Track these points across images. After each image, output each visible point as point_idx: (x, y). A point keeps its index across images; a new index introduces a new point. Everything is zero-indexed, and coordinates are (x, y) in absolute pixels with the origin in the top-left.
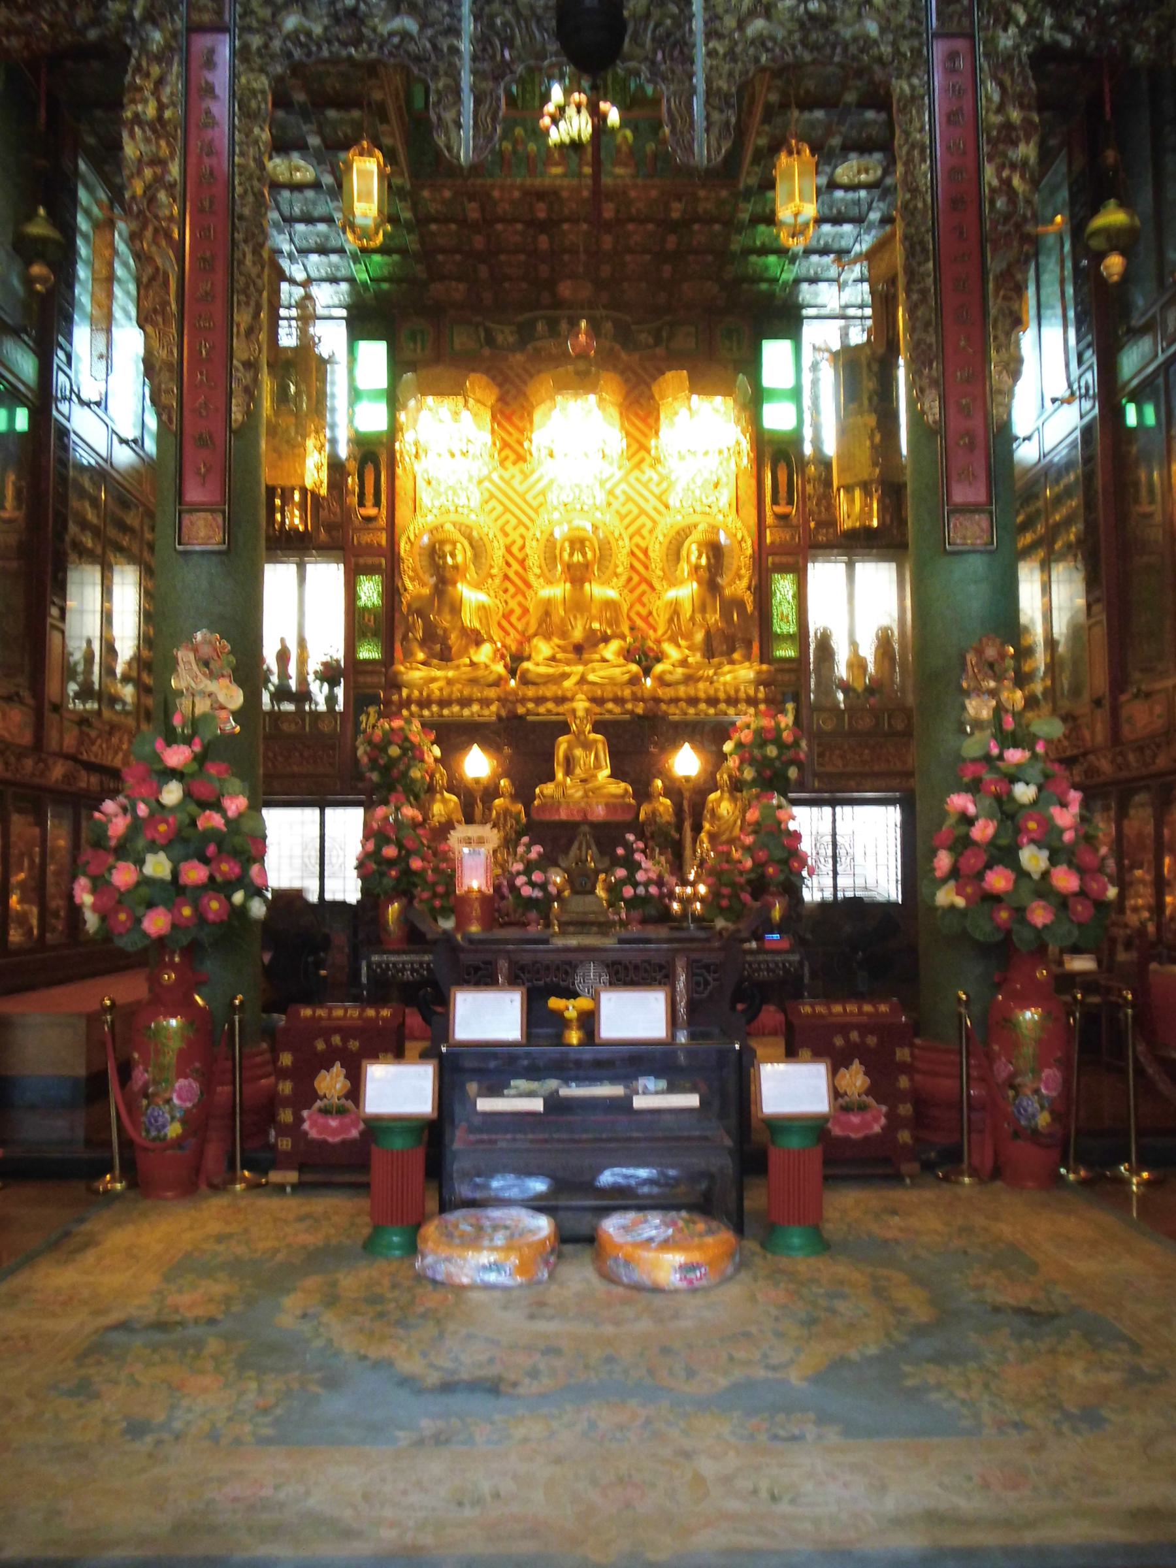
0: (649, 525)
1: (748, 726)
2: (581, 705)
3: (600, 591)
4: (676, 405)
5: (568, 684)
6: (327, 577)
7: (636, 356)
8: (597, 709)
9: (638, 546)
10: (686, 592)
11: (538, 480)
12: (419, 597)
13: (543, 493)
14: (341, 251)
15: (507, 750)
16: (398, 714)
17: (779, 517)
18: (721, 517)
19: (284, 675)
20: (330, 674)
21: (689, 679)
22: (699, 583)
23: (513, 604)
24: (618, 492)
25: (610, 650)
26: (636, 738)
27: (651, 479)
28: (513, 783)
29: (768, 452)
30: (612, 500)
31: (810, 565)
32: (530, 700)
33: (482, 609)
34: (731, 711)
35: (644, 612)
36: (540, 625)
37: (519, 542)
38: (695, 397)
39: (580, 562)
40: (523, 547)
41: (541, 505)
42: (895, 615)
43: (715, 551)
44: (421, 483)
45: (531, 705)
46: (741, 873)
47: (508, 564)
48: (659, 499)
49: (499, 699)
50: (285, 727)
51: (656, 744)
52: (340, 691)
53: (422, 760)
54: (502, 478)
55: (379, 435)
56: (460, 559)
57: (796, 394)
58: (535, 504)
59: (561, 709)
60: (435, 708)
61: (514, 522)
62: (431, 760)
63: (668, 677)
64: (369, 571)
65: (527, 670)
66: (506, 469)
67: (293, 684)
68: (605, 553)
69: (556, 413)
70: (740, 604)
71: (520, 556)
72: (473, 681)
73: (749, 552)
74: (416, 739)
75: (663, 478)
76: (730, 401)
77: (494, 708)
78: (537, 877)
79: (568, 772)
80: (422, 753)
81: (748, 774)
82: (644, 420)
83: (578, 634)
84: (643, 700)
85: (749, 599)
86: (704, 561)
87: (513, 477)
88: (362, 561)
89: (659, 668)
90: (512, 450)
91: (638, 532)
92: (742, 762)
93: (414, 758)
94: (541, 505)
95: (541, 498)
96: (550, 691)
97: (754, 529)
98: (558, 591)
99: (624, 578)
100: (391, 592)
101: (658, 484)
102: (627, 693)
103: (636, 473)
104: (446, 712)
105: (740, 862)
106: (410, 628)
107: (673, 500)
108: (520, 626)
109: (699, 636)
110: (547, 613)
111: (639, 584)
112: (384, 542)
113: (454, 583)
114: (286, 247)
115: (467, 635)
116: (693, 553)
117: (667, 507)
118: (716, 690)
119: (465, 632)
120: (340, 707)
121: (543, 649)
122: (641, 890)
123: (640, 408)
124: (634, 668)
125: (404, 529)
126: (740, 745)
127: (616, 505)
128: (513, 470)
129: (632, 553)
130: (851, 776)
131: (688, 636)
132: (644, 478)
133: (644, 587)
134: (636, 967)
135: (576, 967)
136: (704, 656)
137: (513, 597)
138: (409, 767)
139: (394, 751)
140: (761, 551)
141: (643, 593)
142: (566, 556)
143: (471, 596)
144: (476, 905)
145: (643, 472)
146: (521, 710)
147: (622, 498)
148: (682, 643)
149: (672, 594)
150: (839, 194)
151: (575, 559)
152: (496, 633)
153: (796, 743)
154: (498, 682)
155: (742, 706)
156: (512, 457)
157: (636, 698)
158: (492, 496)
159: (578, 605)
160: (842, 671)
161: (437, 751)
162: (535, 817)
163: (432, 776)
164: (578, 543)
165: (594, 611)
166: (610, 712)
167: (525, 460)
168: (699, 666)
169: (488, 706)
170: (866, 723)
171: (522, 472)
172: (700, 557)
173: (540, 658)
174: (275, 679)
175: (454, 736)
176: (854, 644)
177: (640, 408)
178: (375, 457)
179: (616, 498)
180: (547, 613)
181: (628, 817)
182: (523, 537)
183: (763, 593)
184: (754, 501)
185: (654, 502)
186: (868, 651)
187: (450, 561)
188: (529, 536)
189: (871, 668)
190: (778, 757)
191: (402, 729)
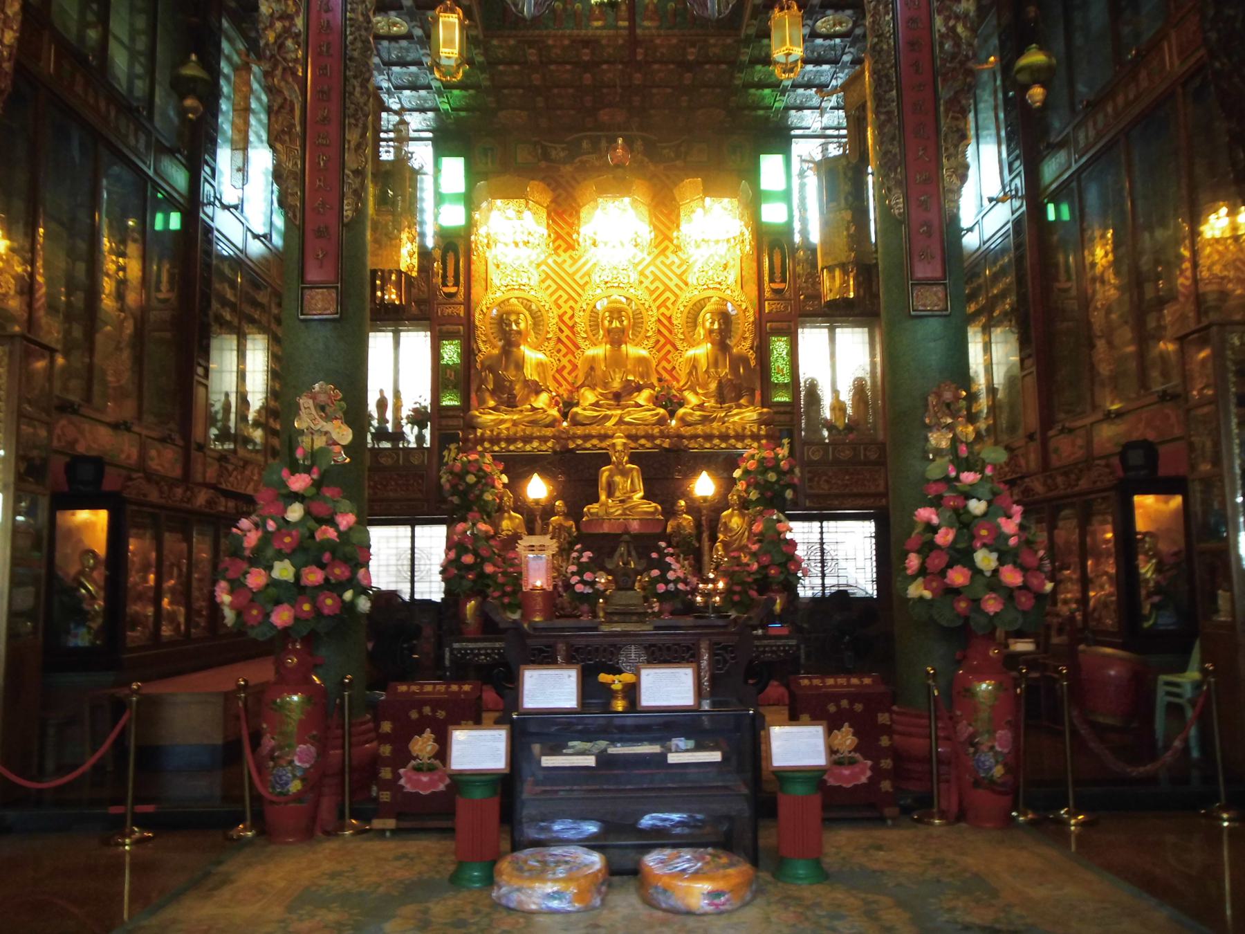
0: (673, 298)
1: (753, 456)
2: (619, 441)
3: (634, 351)
4: (694, 204)
5: (609, 424)
6: (417, 342)
7: (662, 167)
8: (633, 445)
9: (663, 314)
10: (702, 351)
11: (585, 264)
12: (490, 357)
13: (588, 274)
14: (428, 87)
15: (561, 478)
16: (473, 450)
17: (775, 291)
18: (728, 292)
19: (383, 420)
20: (419, 418)
21: (705, 420)
23: (565, 361)
24: (647, 272)
25: (643, 397)
26: (664, 466)
27: (673, 262)
28: (566, 504)
29: (766, 240)
31: (800, 330)
33: (540, 365)
34: (739, 445)
35: (669, 367)
36: (586, 378)
37: (570, 313)
38: (707, 199)
39: (618, 327)
40: (572, 317)
41: (587, 283)
42: (868, 368)
43: (725, 318)
44: (491, 268)
45: (579, 442)
46: (750, 574)
47: (562, 331)
48: (680, 276)
49: (554, 437)
50: (383, 461)
51: (679, 471)
52: (427, 432)
53: (493, 487)
54: (555, 262)
55: (459, 228)
56: (522, 326)
57: (787, 196)
58: (582, 282)
59: (604, 445)
60: (503, 445)
61: (565, 297)
62: (500, 486)
63: (689, 419)
64: (450, 336)
65: (577, 413)
66: (559, 255)
67: (390, 427)
68: (638, 320)
69: (598, 212)
70: (744, 360)
71: (570, 324)
72: (533, 423)
73: (752, 319)
74: (488, 470)
75: (683, 262)
76: (735, 202)
77: (550, 444)
78: (588, 576)
79: (610, 494)
80: (493, 481)
81: (754, 495)
82: (668, 216)
83: (616, 385)
84: (668, 437)
85: (751, 355)
86: (716, 326)
87: (565, 261)
88: (445, 328)
89: (681, 411)
90: (563, 240)
91: (663, 304)
92: (748, 486)
93: (486, 484)
94: (587, 283)
95: (586, 278)
96: (595, 430)
97: (756, 301)
98: (600, 351)
99: (652, 341)
100: (468, 353)
101: (679, 267)
102: (656, 431)
103: (662, 258)
104: (512, 448)
105: (748, 565)
106: (483, 381)
107: (692, 280)
108: (570, 379)
109: (713, 386)
110: (592, 368)
111: (664, 345)
112: (462, 314)
113: (518, 346)
114: (385, 85)
115: (529, 386)
116: (707, 320)
117: (686, 284)
118: (728, 428)
119: (526, 383)
120: (427, 444)
121: (589, 396)
122: (671, 586)
123: (665, 209)
124: (662, 411)
125: (478, 303)
126: (746, 472)
127: (647, 283)
128: (565, 256)
129: (659, 320)
130: (837, 496)
132: (668, 262)
133: (669, 347)
134: (669, 649)
135: (620, 648)
136: (717, 402)
137: (564, 356)
138: (482, 492)
139: (471, 479)
140: (761, 320)
141: (669, 352)
142: (606, 323)
143: (531, 355)
144: (539, 599)
145: (667, 257)
146: (572, 446)
147: (651, 278)
148: (700, 391)
149: (691, 353)
150: (819, 41)
151: (614, 325)
152: (551, 385)
153: (791, 471)
154: (552, 424)
155: (748, 441)
156: (564, 246)
157: (663, 435)
158: (548, 276)
159: (616, 361)
160: (827, 413)
161: (505, 479)
162: (584, 531)
163: (501, 499)
164: (616, 313)
165: (629, 367)
166: (643, 446)
167: (574, 249)
168: (714, 409)
170: (847, 454)
171: (571, 257)
172: (712, 323)
173: (587, 404)
174: (375, 423)
175: (519, 467)
176: (835, 392)
177: (665, 209)
178: (456, 248)
179: (647, 277)
180: (592, 368)
181: (659, 530)
182: (571, 307)
183: (763, 352)
184: (755, 276)
186: (846, 396)
187: (514, 327)
188: (577, 307)
189: (849, 411)
190: (777, 482)
191: (477, 460)
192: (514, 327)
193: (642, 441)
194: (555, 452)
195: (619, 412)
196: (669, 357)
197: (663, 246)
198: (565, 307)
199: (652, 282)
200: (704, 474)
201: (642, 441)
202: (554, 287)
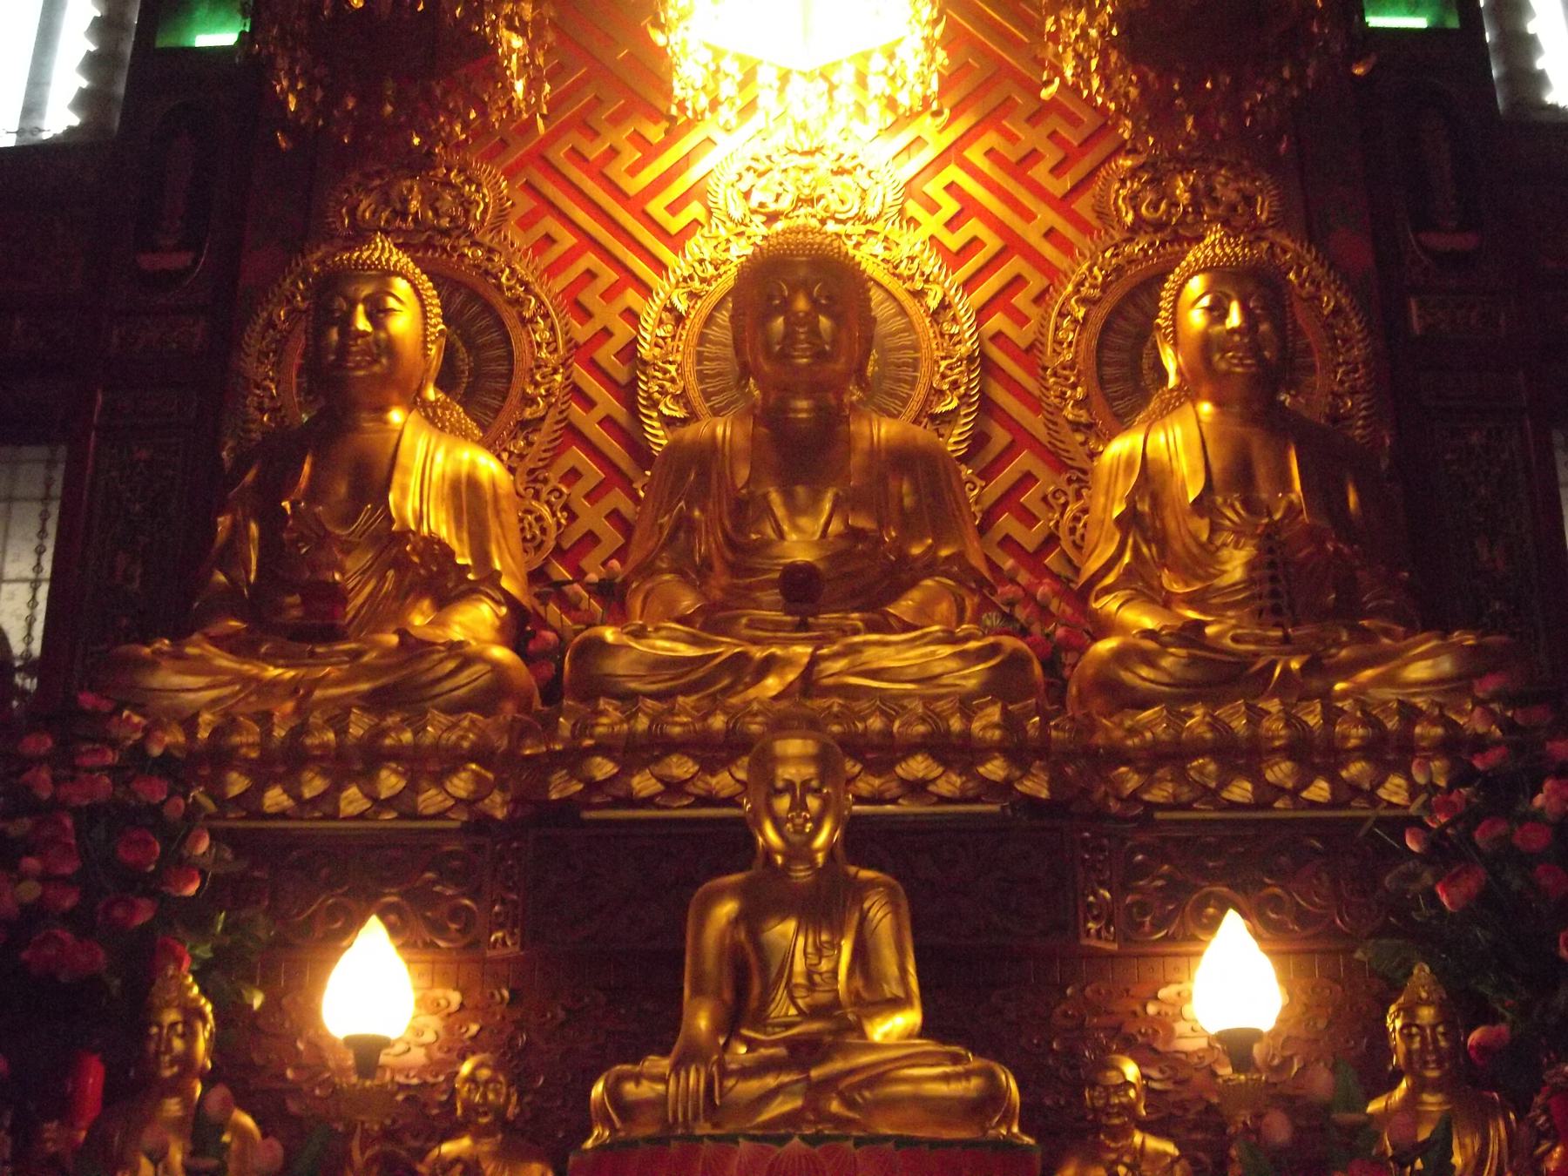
0: (1036, 282)
22: (1218, 403)
23: (592, 518)
30: (913, 209)
32: (604, 748)
35: (1030, 538)
45: (603, 768)
49: (481, 754)
51: (1107, 916)
59: (723, 782)
77: (460, 785)
79: (739, 1014)
86: (1234, 319)
95: (695, 210)
109: (1235, 564)
115: (401, 564)
131: (1202, 562)
137: (593, 496)
141: (1028, 479)
146: (561, 787)
147: (950, 207)
149: (1123, 446)
166: (917, 788)
169: (439, 780)
172: (1217, 311)
179: (933, 208)
185: (1047, 216)
187: (362, 324)
188: (650, 312)
192: (362, 324)
193: (918, 766)
194: (481, 824)
195: (803, 651)
196: (1028, 498)
197: (994, 99)
198: (607, 315)
199: (952, 224)
200: (1233, 925)
201: (918, 766)
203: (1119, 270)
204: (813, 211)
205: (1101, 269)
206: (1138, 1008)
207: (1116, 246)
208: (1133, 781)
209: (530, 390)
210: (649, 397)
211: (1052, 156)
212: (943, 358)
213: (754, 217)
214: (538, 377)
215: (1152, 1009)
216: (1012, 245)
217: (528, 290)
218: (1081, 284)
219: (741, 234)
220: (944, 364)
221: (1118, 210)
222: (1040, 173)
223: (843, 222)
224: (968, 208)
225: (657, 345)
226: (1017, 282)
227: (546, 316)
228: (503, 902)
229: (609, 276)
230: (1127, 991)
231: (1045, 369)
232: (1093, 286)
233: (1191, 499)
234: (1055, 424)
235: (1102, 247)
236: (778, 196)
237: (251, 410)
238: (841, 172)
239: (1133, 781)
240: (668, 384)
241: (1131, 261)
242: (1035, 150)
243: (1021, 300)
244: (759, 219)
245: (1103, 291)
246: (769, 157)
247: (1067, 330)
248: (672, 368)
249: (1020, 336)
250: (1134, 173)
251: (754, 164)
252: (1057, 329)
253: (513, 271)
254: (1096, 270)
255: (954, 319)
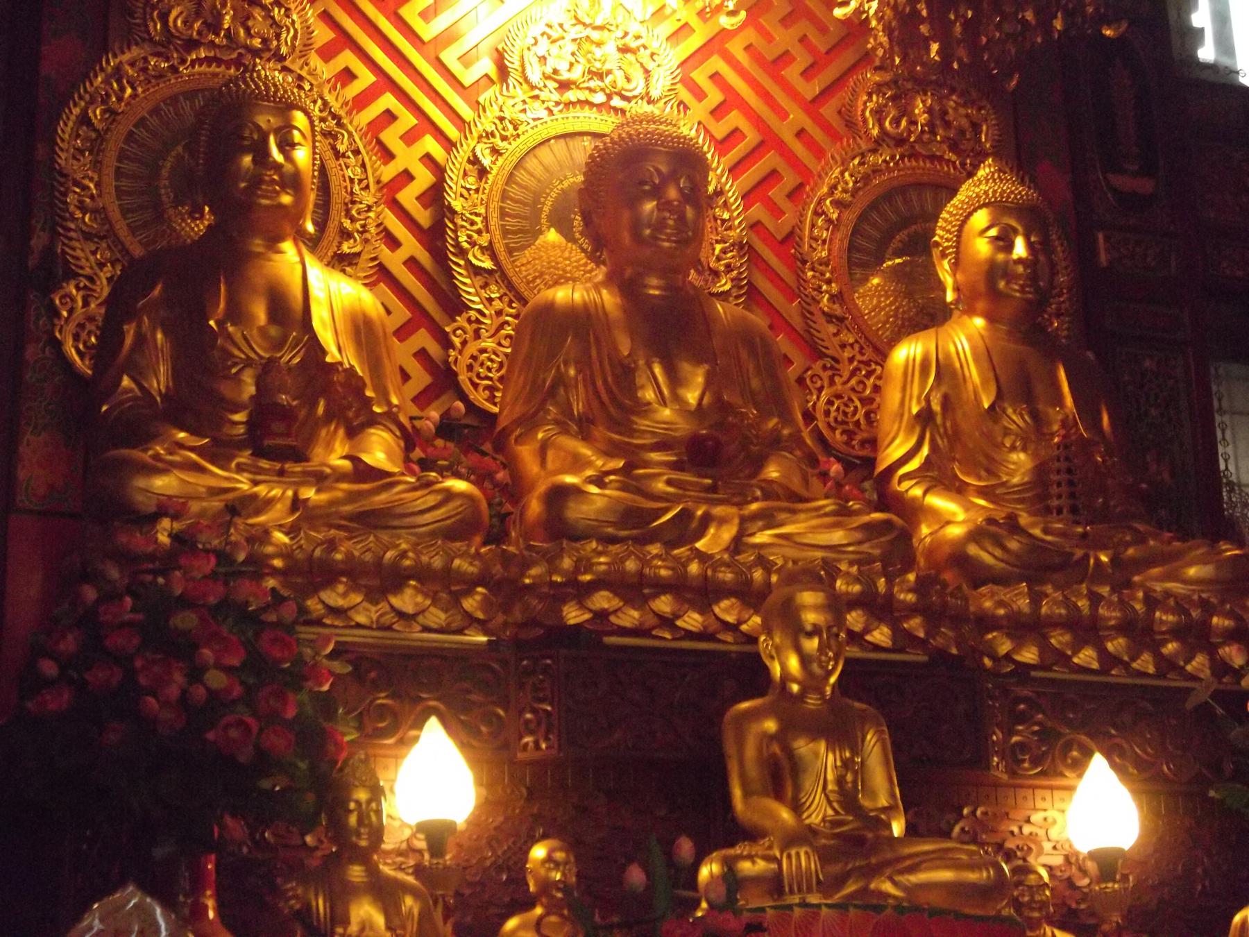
33: (361, 329)
37: (424, 178)
61: (408, 120)
86: (1020, 249)
146: (573, 615)
147: (715, 96)
172: (1004, 242)
179: (699, 94)
185: (797, 116)
198: (408, 157)
199: (718, 112)
200: (1099, 764)
202: (366, 78)
203: (866, 179)
204: (602, 84)
205: (851, 176)
206: (1016, 830)
207: (863, 155)
208: (1005, 647)
209: (347, 224)
210: (457, 245)
211: (802, 60)
212: (717, 242)
213: (549, 83)
214: (354, 212)
215: (1027, 829)
216: (769, 141)
217: (339, 124)
218: (834, 187)
219: (536, 97)
220: (718, 247)
221: (865, 121)
222: (792, 73)
223: (628, 99)
224: (731, 102)
225: (462, 196)
226: (772, 176)
227: (357, 152)
228: (534, 711)
229: (408, 120)
230: (1007, 814)
231: (804, 262)
232: (845, 191)
233: (986, 406)
234: (811, 313)
235: (850, 154)
236: (571, 65)
237: (72, 208)
238: (624, 50)
239: (1005, 647)
240: (475, 236)
241: (876, 171)
242: (787, 53)
243: (777, 193)
244: (552, 85)
245: (853, 196)
246: (561, 26)
247: (821, 228)
248: (478, 220)
249: (779, 227)
250: (879, 88)
251: (548, 30)
252: (813, 226)
253: (325, 103)
254: (847, 174)
255: (726, 205)
